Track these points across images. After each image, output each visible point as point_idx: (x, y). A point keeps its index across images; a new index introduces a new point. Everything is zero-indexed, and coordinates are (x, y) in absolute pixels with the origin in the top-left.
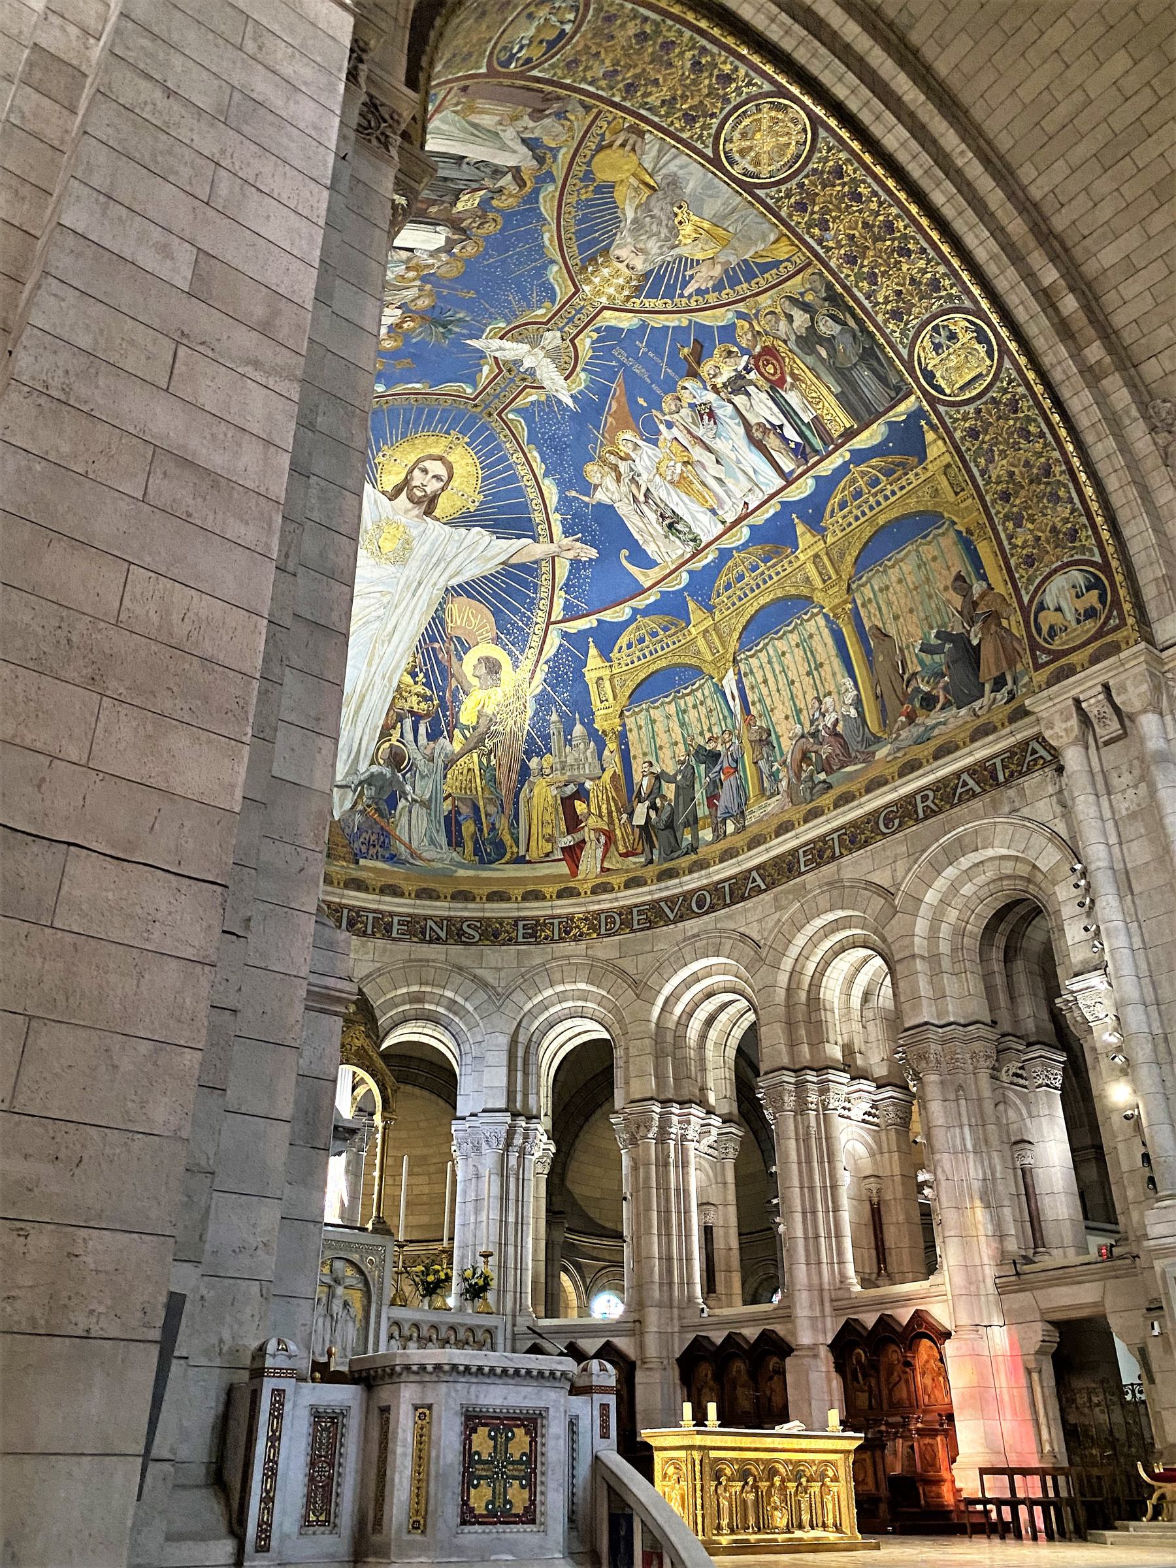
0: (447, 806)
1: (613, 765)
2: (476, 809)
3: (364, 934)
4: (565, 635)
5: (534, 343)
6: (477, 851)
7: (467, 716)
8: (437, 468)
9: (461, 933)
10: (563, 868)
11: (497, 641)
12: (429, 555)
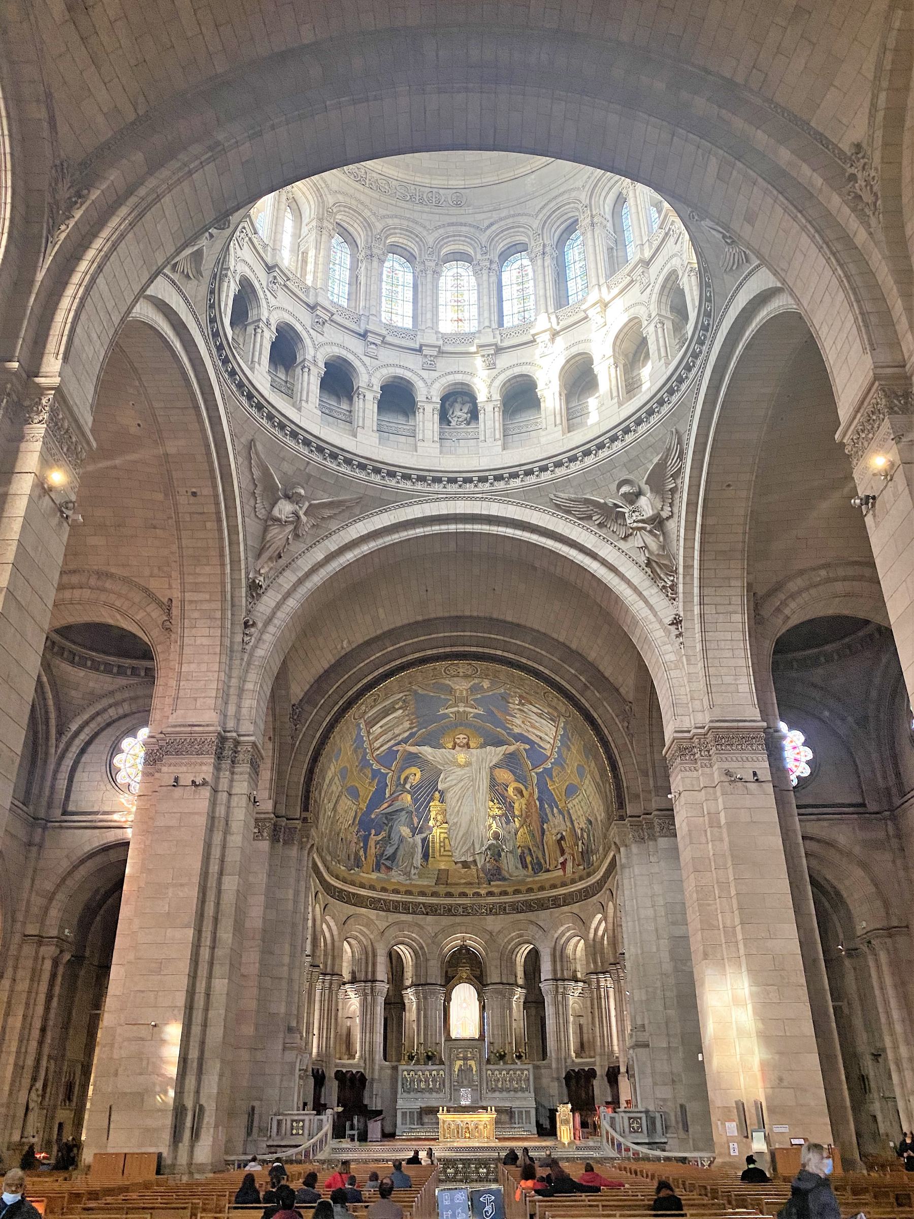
0: (519, 851)
1: (569, 824)
2: (529, 849)
3: (496, 914)
4: (537, 773)
5: (458, 706)
6: (533, 869)
7: (517, 813)
8: (462, 736)
9: (531, 905)
10: (561, 873)
11: (516, 781)
12: (478, 758)
